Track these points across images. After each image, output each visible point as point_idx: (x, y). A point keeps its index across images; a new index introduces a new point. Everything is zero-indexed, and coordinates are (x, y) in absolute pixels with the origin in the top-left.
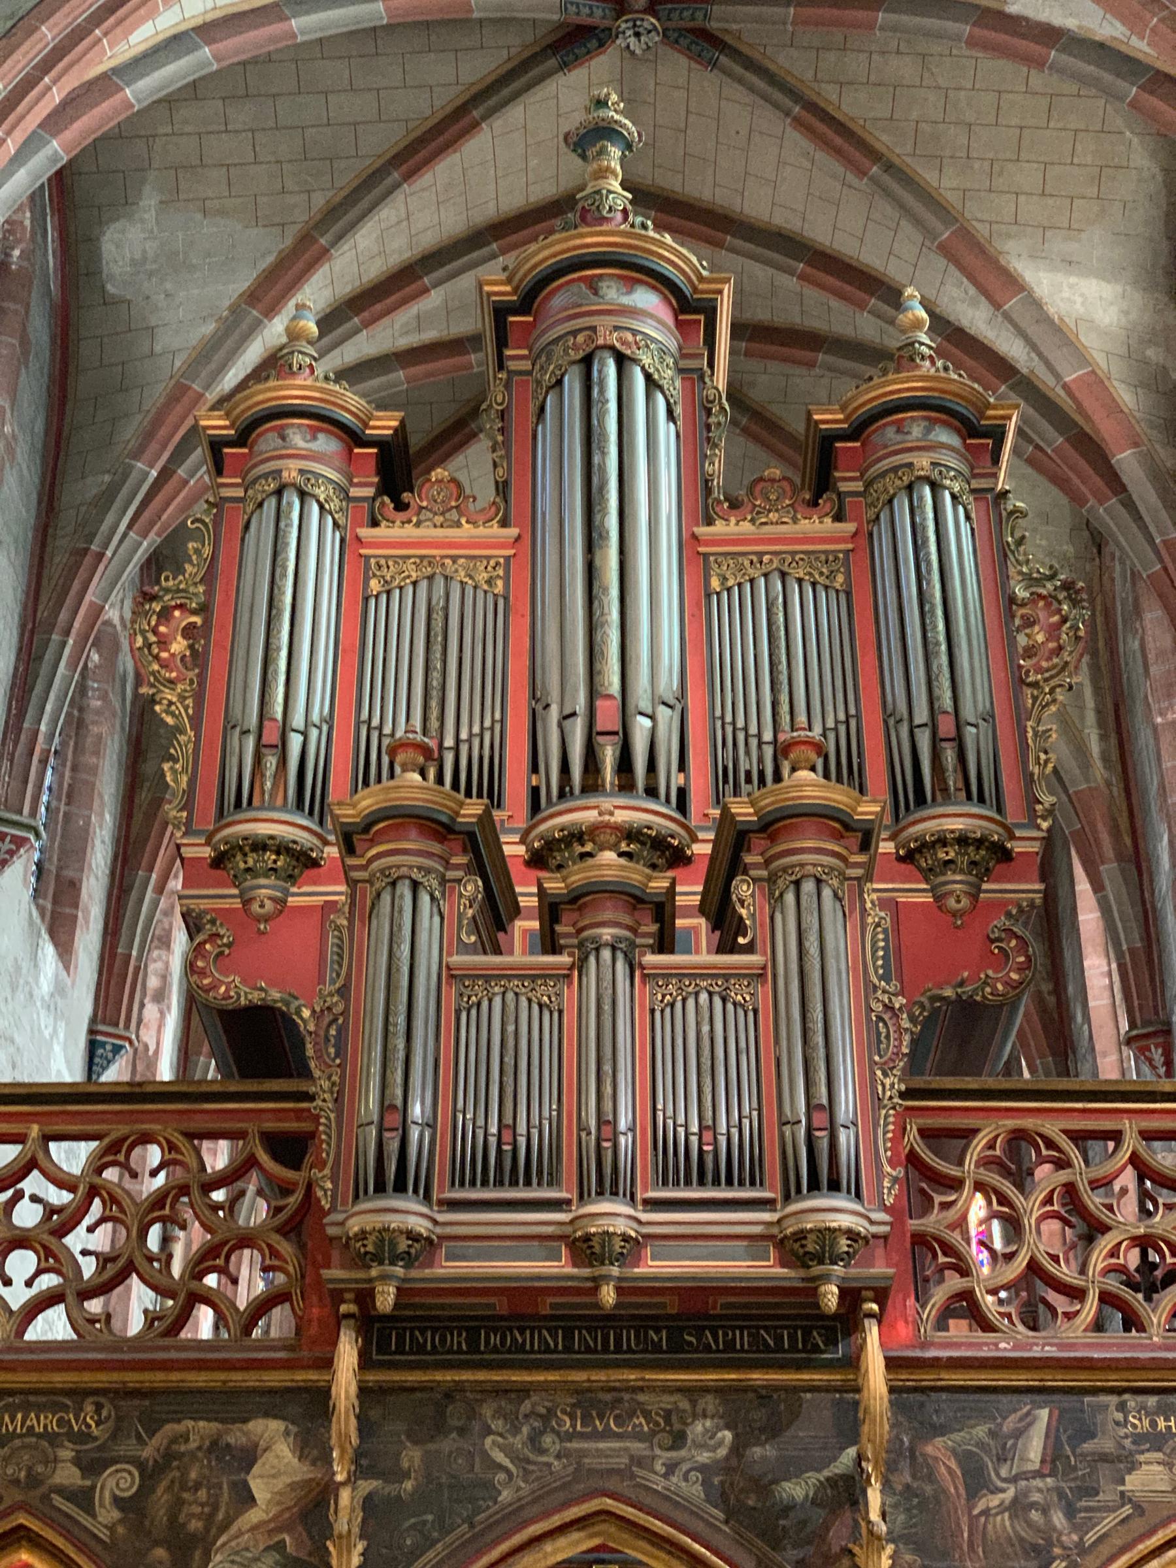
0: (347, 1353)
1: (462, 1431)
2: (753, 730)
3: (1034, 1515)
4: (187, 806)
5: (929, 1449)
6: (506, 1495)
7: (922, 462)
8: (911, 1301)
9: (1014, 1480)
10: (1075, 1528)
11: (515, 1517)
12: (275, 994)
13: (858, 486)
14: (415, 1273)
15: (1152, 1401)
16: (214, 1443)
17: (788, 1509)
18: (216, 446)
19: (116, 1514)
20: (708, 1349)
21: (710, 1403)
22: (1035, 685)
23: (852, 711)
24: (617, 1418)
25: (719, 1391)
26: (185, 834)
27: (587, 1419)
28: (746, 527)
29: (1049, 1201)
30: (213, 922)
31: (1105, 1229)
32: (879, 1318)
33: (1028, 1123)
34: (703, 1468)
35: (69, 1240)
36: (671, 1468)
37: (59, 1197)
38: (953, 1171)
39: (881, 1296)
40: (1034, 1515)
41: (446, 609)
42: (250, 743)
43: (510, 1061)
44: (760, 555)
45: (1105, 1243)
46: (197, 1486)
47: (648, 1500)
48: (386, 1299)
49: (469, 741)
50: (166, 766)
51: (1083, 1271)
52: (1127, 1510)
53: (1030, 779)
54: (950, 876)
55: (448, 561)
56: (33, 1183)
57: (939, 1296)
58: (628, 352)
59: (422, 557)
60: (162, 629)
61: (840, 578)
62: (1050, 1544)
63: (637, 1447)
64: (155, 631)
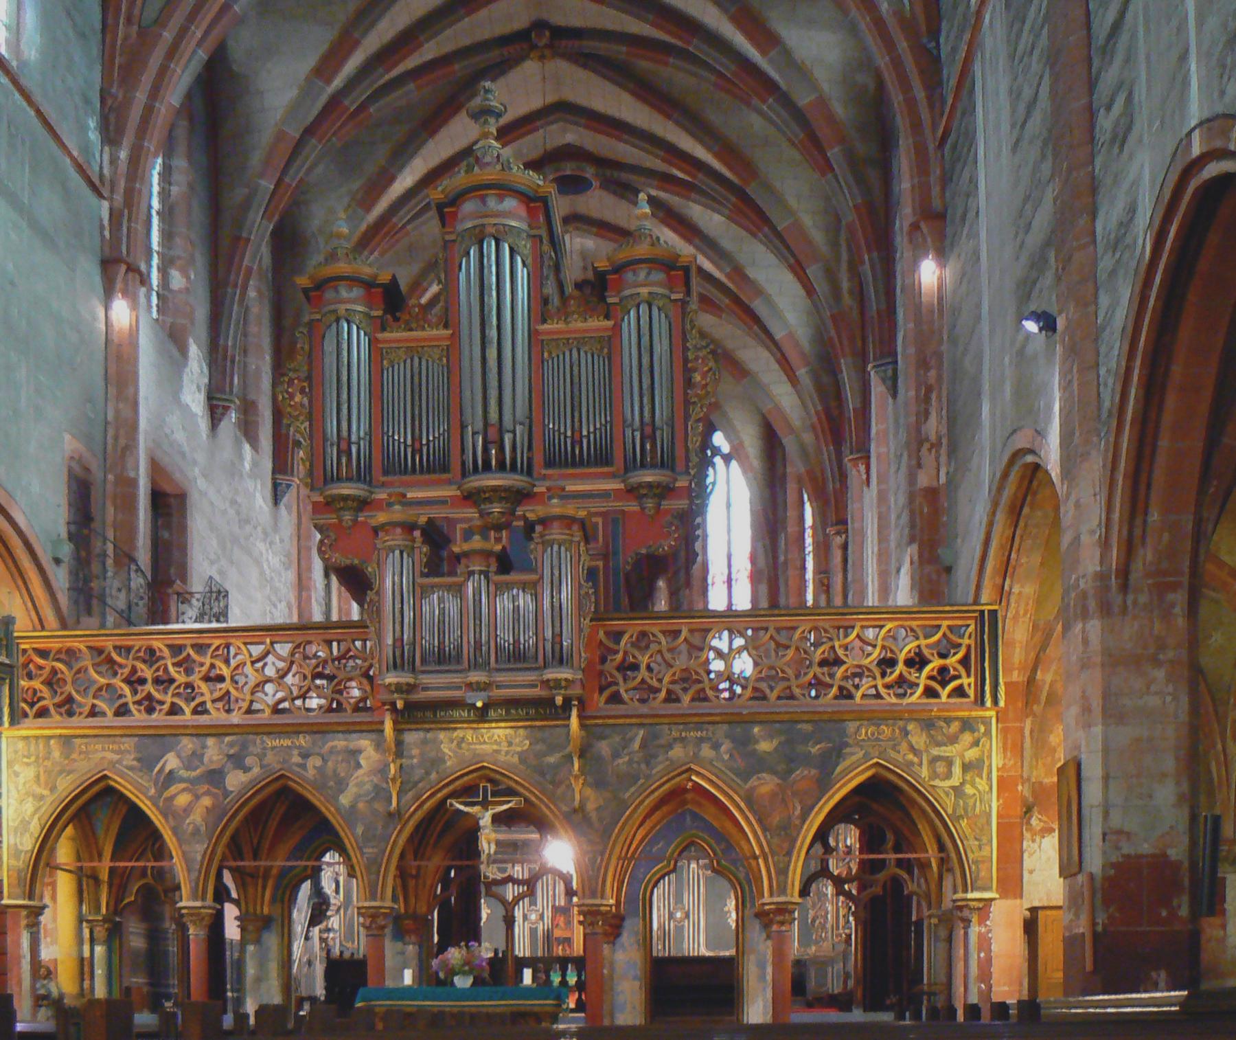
2: (562, 430)
7: (644, 291)
8: (596, 695)
12: (356, 562)
15: (681, 727)
21: (521, 731)
22: (694, 403)
23: (608, 419)
28: (561, 326)
30: (327, 529)
34: (520, 754)
35: (285, 680)
37: (281, 665)
38: (616, 647)
40: (635, 766)
44: (568, 339)
52: (668, 763)
56: (270, 659)
57: (606, 694)
61: (606, 350)
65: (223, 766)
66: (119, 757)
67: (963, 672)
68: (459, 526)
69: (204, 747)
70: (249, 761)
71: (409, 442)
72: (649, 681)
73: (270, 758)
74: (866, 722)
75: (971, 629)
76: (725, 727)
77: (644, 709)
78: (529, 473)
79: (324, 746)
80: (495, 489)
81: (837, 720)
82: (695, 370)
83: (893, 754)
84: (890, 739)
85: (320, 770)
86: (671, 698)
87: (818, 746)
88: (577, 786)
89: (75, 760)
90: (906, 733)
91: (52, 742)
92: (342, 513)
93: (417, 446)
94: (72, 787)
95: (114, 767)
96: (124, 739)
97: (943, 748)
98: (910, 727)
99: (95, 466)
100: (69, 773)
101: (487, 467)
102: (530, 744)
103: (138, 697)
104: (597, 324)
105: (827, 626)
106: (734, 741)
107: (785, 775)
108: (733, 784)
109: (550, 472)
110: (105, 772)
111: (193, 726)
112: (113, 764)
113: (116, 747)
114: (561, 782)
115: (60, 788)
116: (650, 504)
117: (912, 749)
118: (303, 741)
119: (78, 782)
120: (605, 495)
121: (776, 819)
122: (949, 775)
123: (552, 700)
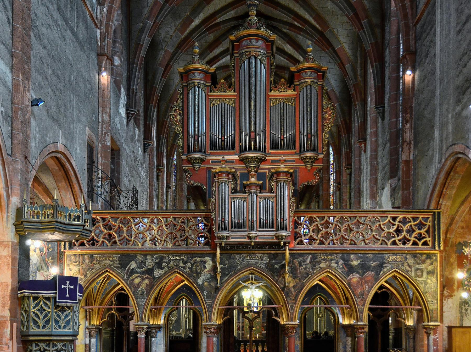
0: (218, 251)
1: (233, 259)
3: (308, 269)
4: (183, 149)
5: (295, 261)
6: (239, 267)
8: (294, 241)
9: (305, 265)
10: (312, 271)
11: (240, 270)
13: (298, 83)
14: (227, 241)
15: (324, 254)
16: (201, 260)
17: (276, 268)
18: (181, 74)
19: (189, 270)
20: (266, 249)
21: (266, 255)
22: (326, 126)
24: (254, 257)
25: (267, 253)
26: (183, 155)
27: (250, 257)
28: (277, 93)
29: (314, 227)
31: (321, 231)
32: (289, 246)
33: (312, 215)
34: (265, 264)
36: (261, 264)
39: (289, 243)
40: (308, 269)
41: (224, 110)
42: (193, 139)
43: (239, 210)
44: (280, 98)
45: (321, 233)
46: (199, 266)
47: (258, 268)
48: (223, 244)
49: (229, 137)
50: (178, 141)
51: (317, 237)
52: (320, 268)
53: (323, 143)
54: (308, 164)
55: (225, 100)
57: (298, 240)
58: (257, 57)
59: (220, 99)
60: (175, 114)
62: (309, 273)
63: (257, 261)
64: (174, 114)
65: (154, 267)
66: (112, 262)
67: (427, 236)
68: (238, 171)
69: (146, 259)
70: (163, 265)
71: (220, 137)
72: (313, 236)
73: (171, 264)
74: (391, 254)
75: (430, 219)
76: (341, 254)
77: (311, 247)
78: (265, 152)
79: (192, 258)
80: (252, 158)
81: (381, 252)
82: (326, 113)
83: (402, 267)
84: (401, 261)
85: (191, 269)
86: (322, 243)
87: (374, 263)
88: (287, 276)
89: (94, 264)
90: (406, 259)
91: (85, 256)
92: (194, 165)
93: (223, 139)
94: (93, 275)
95: (110, 266)
96: (114, 256)
97: (420, 265)
98: (408, 257)
99: (95, 139)
100: (92, 269)
101: (250, 149)
102: (269, 260)
103: (120, 238)
104: (290, 92)
105: (378, 216)
106: (344, 261)
107: (362, 275)
108: (343, 277)
109: (272, 151)
110: (107, 269)
111: (143, 251)
112: (110, 266)
113: (111, 259)
114: (281, 275)
115: (88, 276)
116: (309, 165)
117: (409, 266)
118: (183, 257)
119: (96, 273)
120: (292, 161)
121: (359, 291)
122: (422, 276)
123: (279, 244)
